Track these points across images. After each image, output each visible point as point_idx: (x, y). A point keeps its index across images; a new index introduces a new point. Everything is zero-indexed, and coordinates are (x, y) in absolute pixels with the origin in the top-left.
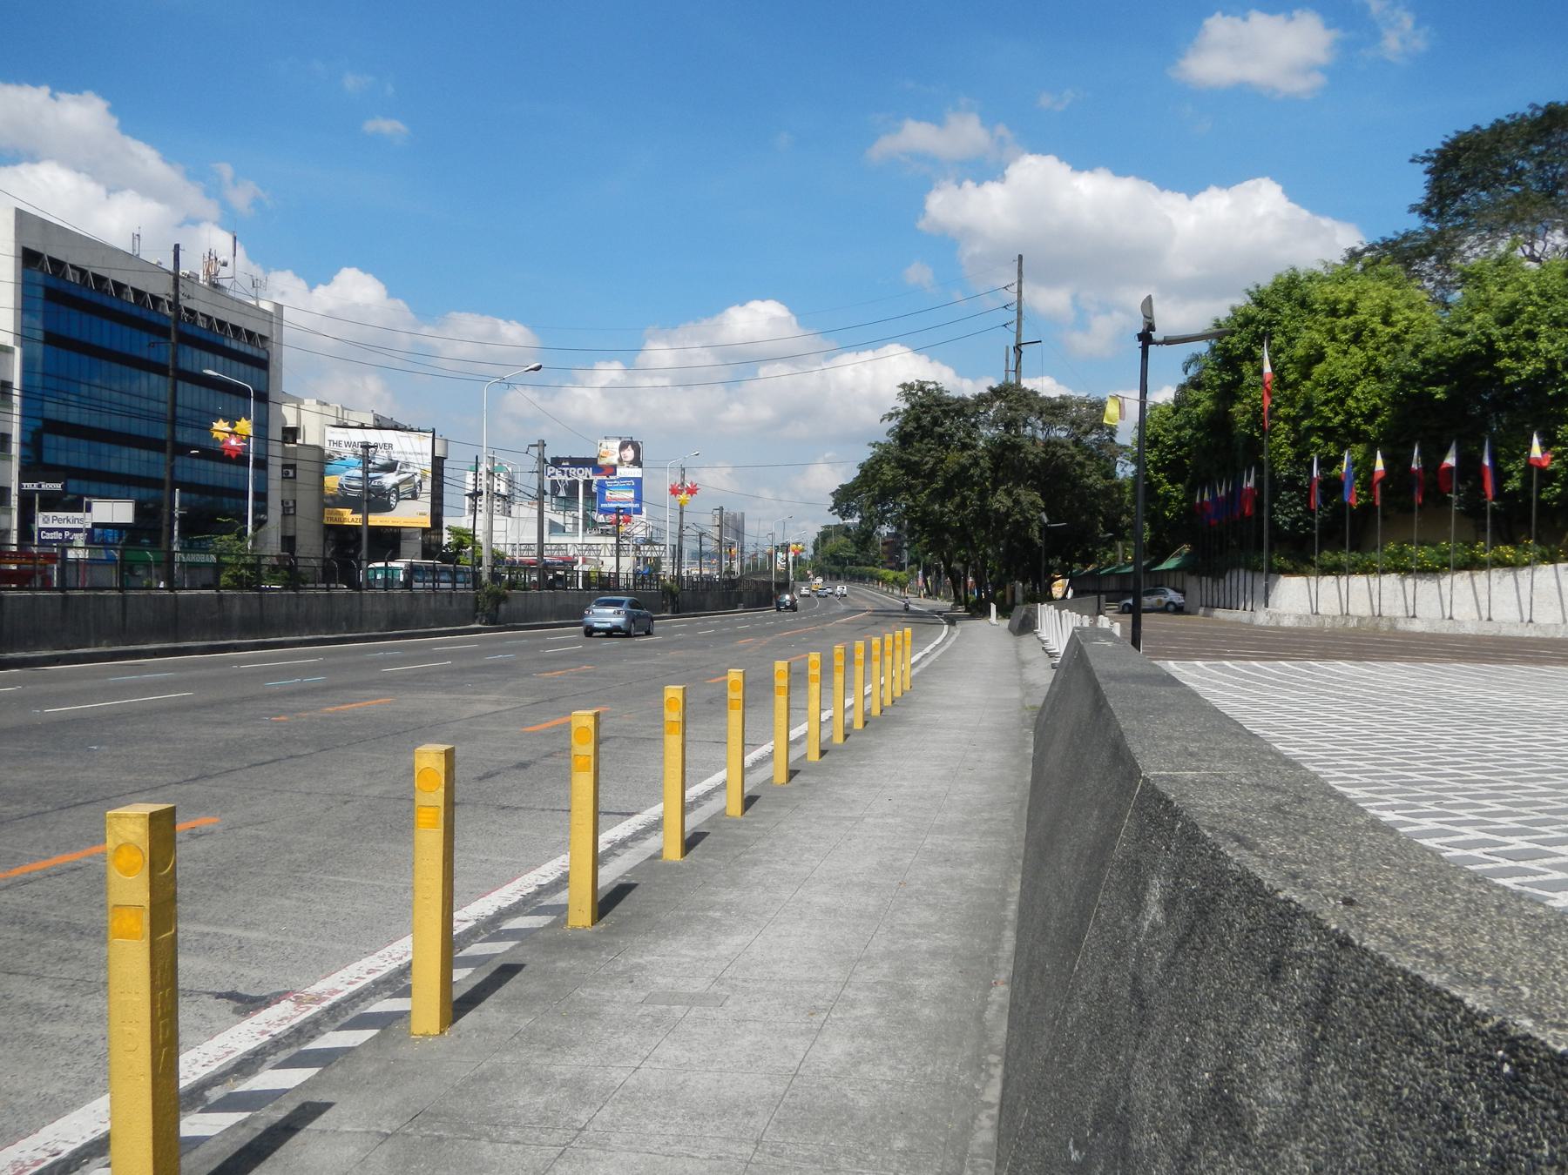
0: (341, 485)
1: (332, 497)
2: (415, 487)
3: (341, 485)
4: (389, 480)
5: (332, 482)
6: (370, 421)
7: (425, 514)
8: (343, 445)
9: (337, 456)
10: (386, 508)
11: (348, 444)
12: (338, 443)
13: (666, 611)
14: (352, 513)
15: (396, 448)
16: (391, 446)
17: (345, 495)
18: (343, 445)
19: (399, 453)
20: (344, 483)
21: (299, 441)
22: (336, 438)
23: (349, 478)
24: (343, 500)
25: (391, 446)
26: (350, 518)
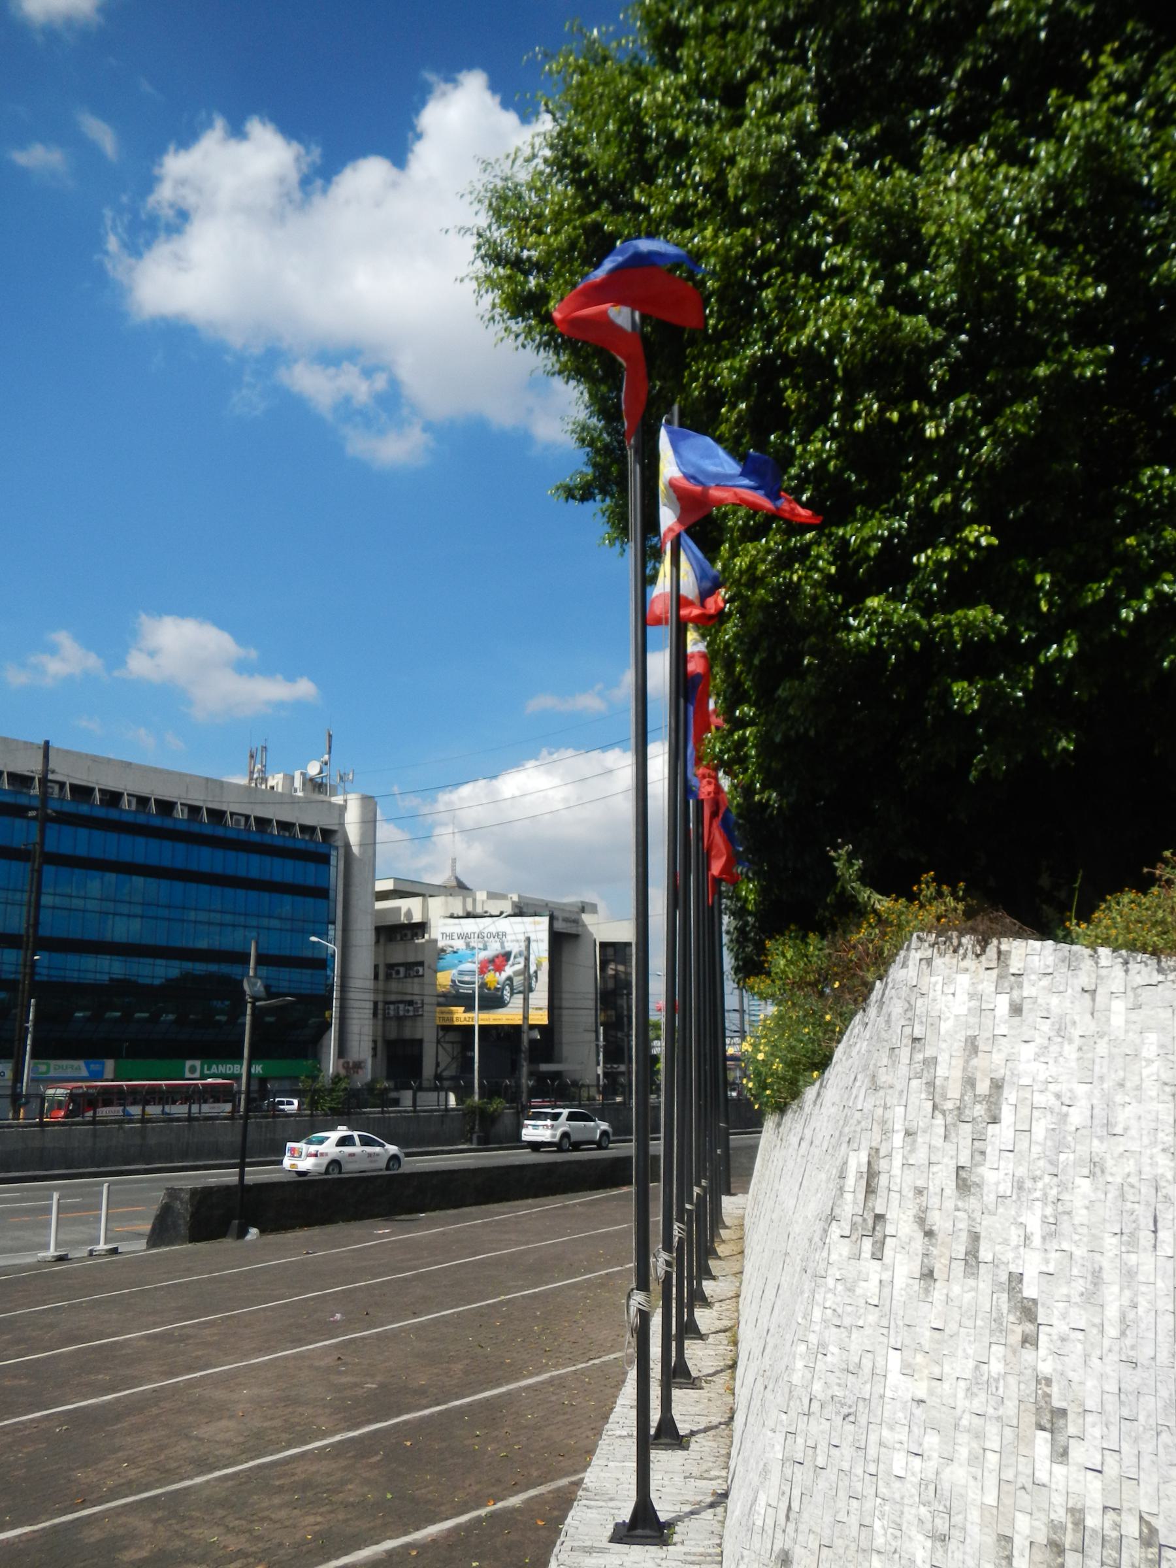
0: (453, 981)
1: (444, 995)
3: (453, 981)
5: (444, 979)
6: (507, 907)
7: (540, 1009)
8: (455, 937)
11: (460, 936)
12: (451, 936)
13: (470, 1141)
14: (465, 1012)
17: (457, 991)
18: (455, 937)
19: (512, 941)
21: (427, 936)
22: (448, 930)
23: (461, 973)
25: (504, 934)
26: (460, 1016)
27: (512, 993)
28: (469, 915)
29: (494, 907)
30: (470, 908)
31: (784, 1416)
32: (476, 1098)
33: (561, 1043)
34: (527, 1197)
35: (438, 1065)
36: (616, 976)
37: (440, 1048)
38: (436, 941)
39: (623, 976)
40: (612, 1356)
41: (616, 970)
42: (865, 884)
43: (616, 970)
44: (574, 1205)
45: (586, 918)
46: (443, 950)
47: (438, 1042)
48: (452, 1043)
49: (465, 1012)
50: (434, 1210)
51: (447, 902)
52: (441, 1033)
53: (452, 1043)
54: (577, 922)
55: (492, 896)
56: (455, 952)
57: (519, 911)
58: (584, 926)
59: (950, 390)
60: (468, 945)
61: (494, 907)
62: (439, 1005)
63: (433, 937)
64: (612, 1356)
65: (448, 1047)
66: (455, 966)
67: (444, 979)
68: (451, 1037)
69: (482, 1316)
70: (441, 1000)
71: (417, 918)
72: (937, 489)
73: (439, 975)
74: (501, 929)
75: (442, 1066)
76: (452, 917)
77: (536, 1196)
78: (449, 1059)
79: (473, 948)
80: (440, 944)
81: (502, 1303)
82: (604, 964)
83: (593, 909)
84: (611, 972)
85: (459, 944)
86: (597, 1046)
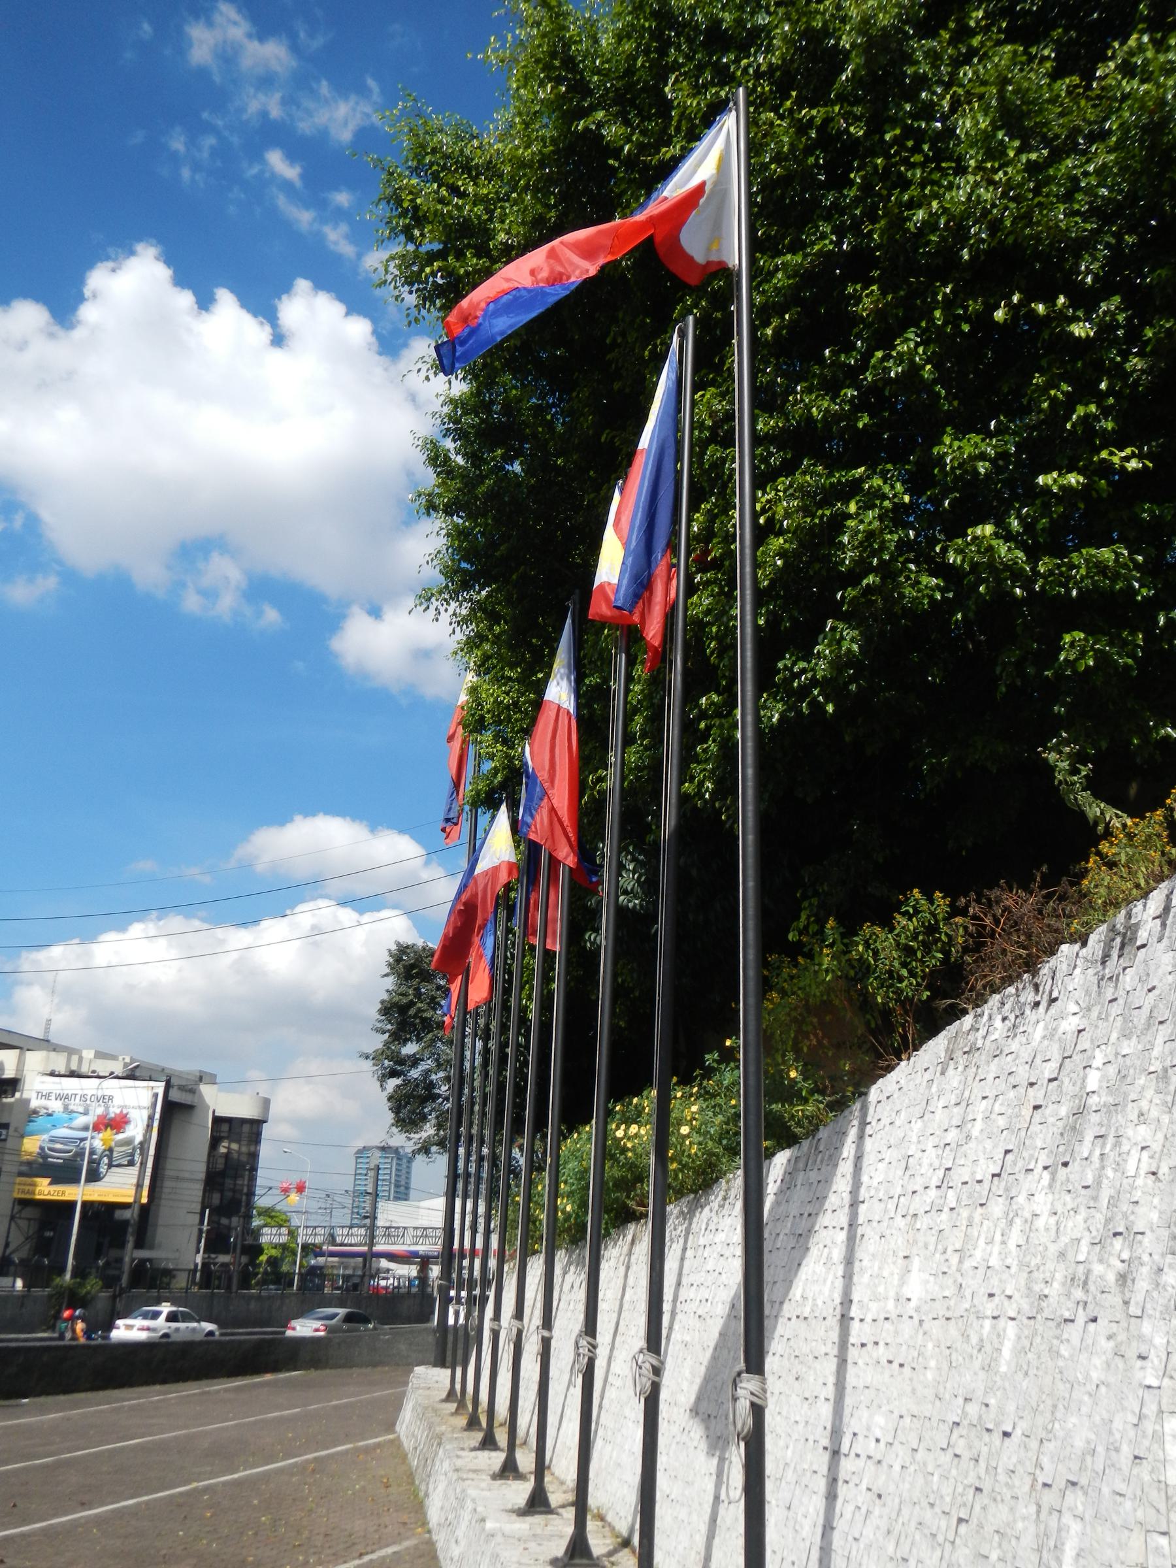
0: (42, 1148)
1: (29, 1163)
2: (134, 1149)
4: (98, 1142)
8: (53, 1097)
9: (43, 1111)
10: (94, 1176)
11: (59, 1097)
12: (47, 1096)
14: (51, 1184)
15: (117, 1101)
16: (111, 1098)
18: (53, 1097)
20: (46, 1146)
21: (17, 1095)
24: (43, 1167)
25: (111, 1098)
26: (45, 1189)
27: (110, 1166)
28: (73, 1074)
29: (103, 1067)
30: (74, 1067)
31: (1163, 1541)
32: (68, 1276)
33: (156, 1225)
34: (154, 1383)
35: (7, 1245)
36: (227, 1156)
37: (13, 1224)
38: (28, 1101)
39: (235, 1156)
40: (390, 1550)
41: (228, 1148)
42: (1097, 795)
43: (228, 1148)
44: (218, 1391)
45: (206, 1090)
46: (35, 1112)
47: (12, 1218)
48: (29, 1220)
49: (51, 1184)
50: (39, 1395)
51: (48, 1058)
52: (17, 1208)
53: (29, 1220)
54: (193, 1091)
55: (99, 1055)
56: (50, 1115)
57: (131, 1075)
58: (201, 1096)
59: (1105, 288)
60: (66, 1107)
61: (103, 1067)
62: (21, 1174)
63: (25, 1096)
64: (390, 1550)
65: (23, 1224)
66: (46, 1131)
67: (31, 1145)
68: (29, 1212)
69: (180, 1506)
70: (24, 1168)
71: (9, 1074)
72: (1070, 403)
73: (26, 1140)
74: (107, 1093)
75: (12, 1247)
76: (52, 1074)
77: (164, 1382)
78: (22, 1239)
79: (72, 1112)
80: (34, 1103)
81: (206, 1489)
82: (215, 1142)
83: (212, 1080)
84: (223, 1150)
85: (56, 1106)
86: (201, 1231)
